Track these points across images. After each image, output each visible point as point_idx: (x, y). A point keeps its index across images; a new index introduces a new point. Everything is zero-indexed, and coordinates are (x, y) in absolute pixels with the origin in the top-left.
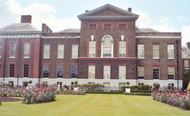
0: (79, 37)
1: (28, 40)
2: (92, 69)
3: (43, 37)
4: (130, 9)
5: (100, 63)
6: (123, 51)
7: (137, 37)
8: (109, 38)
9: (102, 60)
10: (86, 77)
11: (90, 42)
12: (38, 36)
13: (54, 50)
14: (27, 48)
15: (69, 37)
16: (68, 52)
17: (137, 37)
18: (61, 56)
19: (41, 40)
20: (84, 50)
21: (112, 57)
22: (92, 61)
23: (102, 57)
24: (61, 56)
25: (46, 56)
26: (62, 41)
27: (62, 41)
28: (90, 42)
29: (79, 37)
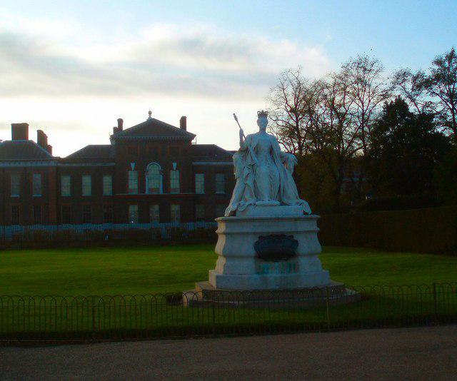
0: (114, 164)
1: (37, 170)
2: (133, 209)
3: (59, 165)
4: (183, 121)
5: (145, 201)
6: (175, 183)
7: (194, 163)
8: (155, 166)
9: (148, 197)
10: (127, 222)
11: (130, 173)
12: (52, 164)
13: (76, 184)
14: (37, 179)
15: (99, 165)
16: (97, 185)
17: (194, 163)
18: (87, 191)
19: (58, 168)
20: (120, 183)
21: (161, 192)
22: (133, 199)
23: (147, 192)
24: (87, 191)
25: (66, 191)
26: (87, 171)
27: (87, 171)
28: (130, 173)
29: (114, 164)
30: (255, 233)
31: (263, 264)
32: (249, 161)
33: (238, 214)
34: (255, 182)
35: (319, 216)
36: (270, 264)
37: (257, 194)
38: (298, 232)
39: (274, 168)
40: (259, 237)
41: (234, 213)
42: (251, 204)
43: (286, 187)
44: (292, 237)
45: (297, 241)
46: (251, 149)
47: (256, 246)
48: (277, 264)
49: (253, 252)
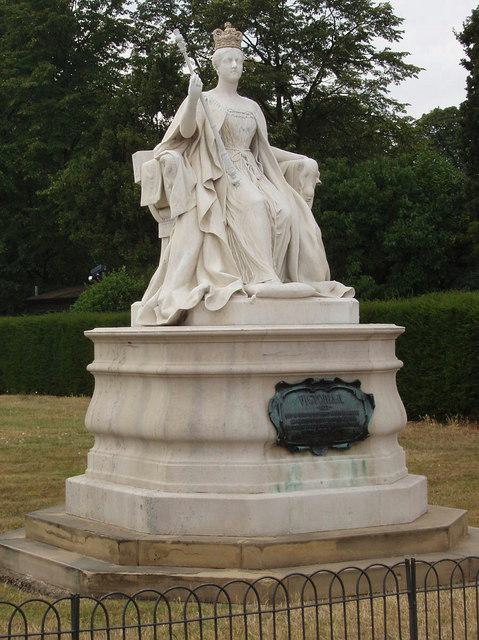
30: (264, 376)
31: (288, 462)
32: (208, 173)
33: (197, 317)
34: (227, 226)
35: (402, 329)
36: (304, 462)
37: (242, 263)
38: (369, 372)
39: (266, 185)
40: (280, 387)
41: (183, 318)
42: (239, 292)
43: (306, 241)
44: (357, 384)
45: (370, 399)
46: (213, 134)
47: (274, 407)
48: (321, 461)
49: (266, 430)
